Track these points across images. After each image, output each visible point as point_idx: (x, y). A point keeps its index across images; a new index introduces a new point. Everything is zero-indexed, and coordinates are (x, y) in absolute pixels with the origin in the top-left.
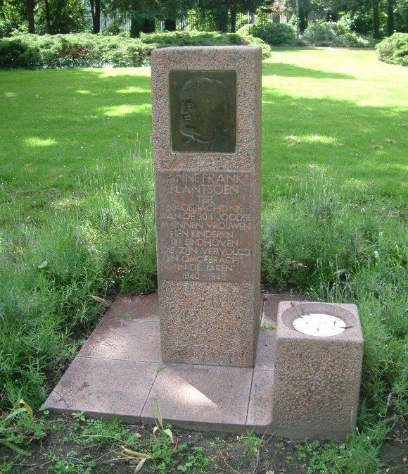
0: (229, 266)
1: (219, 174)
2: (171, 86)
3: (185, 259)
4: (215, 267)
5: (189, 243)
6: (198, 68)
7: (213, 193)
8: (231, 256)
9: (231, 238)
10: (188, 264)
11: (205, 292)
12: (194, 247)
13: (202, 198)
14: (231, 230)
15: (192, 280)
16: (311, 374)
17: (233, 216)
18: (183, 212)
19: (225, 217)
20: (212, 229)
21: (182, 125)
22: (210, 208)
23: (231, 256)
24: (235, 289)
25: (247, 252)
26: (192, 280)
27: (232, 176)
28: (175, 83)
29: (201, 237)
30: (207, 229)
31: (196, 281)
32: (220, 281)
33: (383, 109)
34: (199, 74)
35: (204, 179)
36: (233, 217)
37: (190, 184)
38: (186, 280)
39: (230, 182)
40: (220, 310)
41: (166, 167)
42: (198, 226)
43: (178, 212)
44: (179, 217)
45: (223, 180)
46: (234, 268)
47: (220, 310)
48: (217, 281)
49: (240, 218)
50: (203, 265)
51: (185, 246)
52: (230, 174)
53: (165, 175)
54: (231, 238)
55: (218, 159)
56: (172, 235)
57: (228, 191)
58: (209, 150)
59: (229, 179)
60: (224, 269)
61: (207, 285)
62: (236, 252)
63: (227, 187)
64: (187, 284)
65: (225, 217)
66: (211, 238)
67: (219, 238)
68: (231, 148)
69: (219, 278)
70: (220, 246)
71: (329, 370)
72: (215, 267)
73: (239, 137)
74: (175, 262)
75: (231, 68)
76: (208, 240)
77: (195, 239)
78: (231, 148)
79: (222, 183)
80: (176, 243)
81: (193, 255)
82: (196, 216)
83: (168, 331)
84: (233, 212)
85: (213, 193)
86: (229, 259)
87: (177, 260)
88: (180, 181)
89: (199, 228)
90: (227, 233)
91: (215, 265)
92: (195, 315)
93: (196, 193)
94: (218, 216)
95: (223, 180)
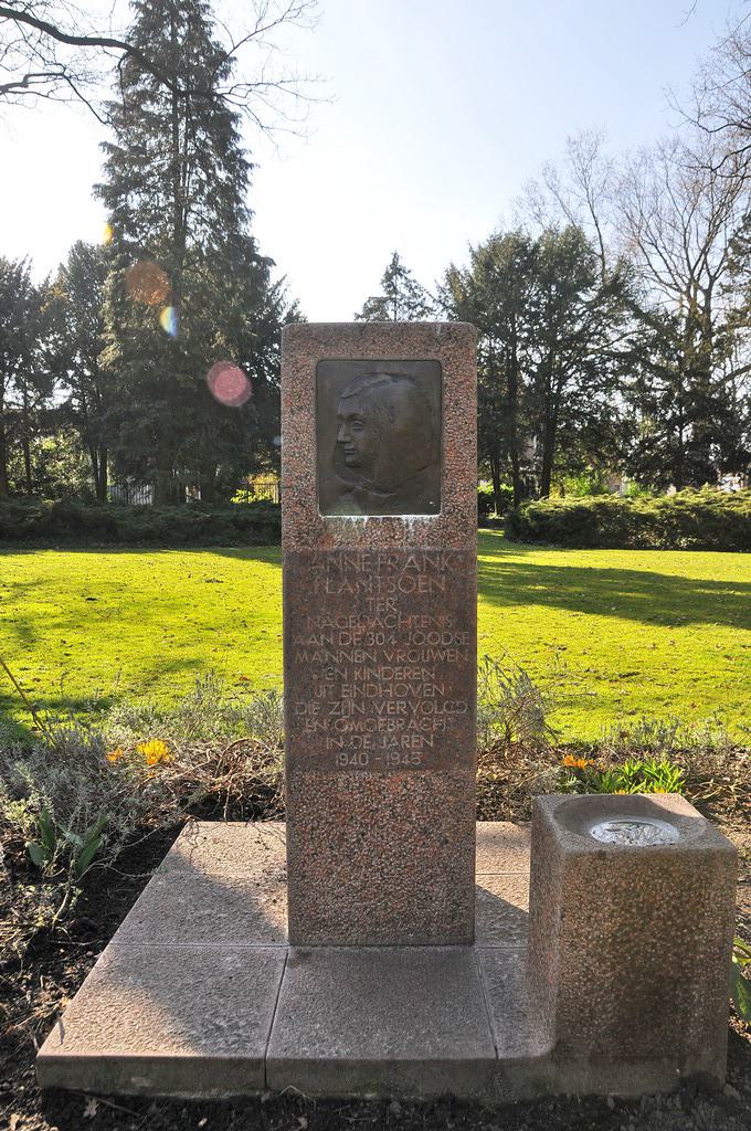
0: (427, 737)
1: (409, 554)
3: (341, 725)
5: (349, 695)
7: (397, 592)
8: (431, 716)
9: (431, 681)
10: (347, 736)
11: (379, 792)
12: (358, 701)
13: (374, 603)
15: (353, 768)
16: (635, 930)
17: (434, 636)
18: (339, 630)
19: (420, 639)
20: (394, 664)
22: (391, 621)
23: (431, 716)
24: (437, 782)
25: (462, 707)
26: (353, 768)
27: (434, 559)
29: (374, 680)
30: (385, 662)
31: (361, 769)
32: (408, 768)
36: (434, 638)
37: (352, 576)
38: (341, 769)
39: (430, 570)
40: (408, 827)
41: (307, 543)
42: (368, 659)
43: (327, 631)
44: (331, 640)
45: (417, 566)
47: (408, 827)
48: (402, 768)
49: (447, 638)
50: (376, 738)
51: (341, 700)
52: (429, 553)
54: (431, 681)
56: (315, 677)
57: (426, 587)
60: (413, 742)
61: (384, 777)
62: (439, 709)
63: (423, 580)
64: (342, 778)
66: (393, 681)
67: (407, 681)
69: (407, 762)
70: (410, 697)
71: (670, 918)
72: (399, 740)
76: (386, 686)
79: (415, 573)
80: (323, 693)
81: (357, 716)
83: (304, 877)
84: (435, 628)
85: (397, 592)
86: (427, 722)
87: (325, 728)
88: (335, 570)
89: (368, 663)
90: (423, 670)
91: (398, 734)
92: (358, 841)
95: (417, 566)
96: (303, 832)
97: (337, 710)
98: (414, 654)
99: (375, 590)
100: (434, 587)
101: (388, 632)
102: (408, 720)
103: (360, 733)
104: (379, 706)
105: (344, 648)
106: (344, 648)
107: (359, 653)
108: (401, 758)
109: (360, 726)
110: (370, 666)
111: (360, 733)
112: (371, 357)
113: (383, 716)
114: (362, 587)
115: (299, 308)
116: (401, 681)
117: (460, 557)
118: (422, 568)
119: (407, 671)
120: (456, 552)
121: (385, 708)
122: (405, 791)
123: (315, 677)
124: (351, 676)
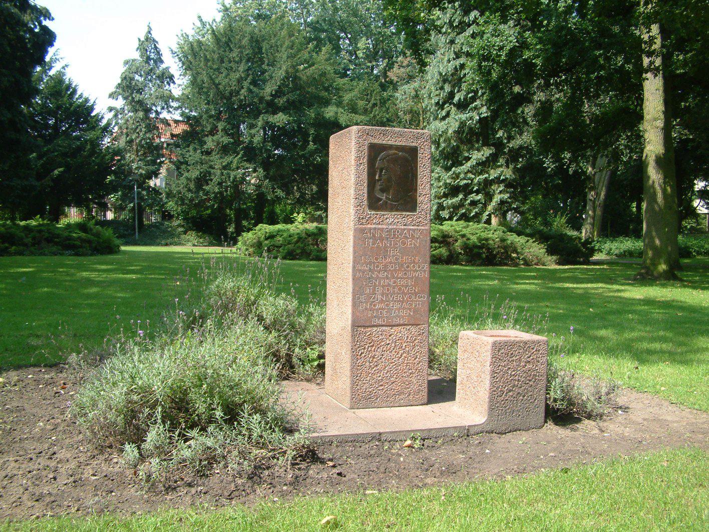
0: (410, 309)
2: (369, 156)
3: (374, 306)
5: (379, 290)
6: (390, 143)
7: (399, 246)
10: (377, 310)
14: (412, 278)
19: (408, 267)
21: (378, 187)
28: (372, 154)
29: (389, 285)
30: (394, 277)
33: (206, 246)
34: (391, 147)
35: (393, 234)
37: (381, 239)
42: (387, 275)
43: (370, 263)
45: (408, 235)
46: (414, 312)
51: (375, 294)
53: (362, 231)
55: (404, 217)
56: (364, 283)
58: (397, 210)
59: (412, 234)
65: (408, 267)
66: (397, 285)
67: (403, 286)
68: (413, 209)
73: (419, 199)
74: (366, 309)
75: (414, 144)
77: (383, 287)
78: (413, 209)
79: (406, 237)
80: (368, 291)
82: (386, 266)
89: (387, 278)
93: (386, 247)
94: (402, 265)
95: (408, 235)
96: (357, 355)
99: (391, 245)
100: (414, 244)
101: (395, 263)
102: (403, 303)
104: (391, 296)
105: (377, 271)
106: (377, 271)
111: (382, 309)
114: (385, 244)
115: (67, 70)
121: (393, 298)
122: (401, 335)
123: (364, 283)
124: (380, 283)
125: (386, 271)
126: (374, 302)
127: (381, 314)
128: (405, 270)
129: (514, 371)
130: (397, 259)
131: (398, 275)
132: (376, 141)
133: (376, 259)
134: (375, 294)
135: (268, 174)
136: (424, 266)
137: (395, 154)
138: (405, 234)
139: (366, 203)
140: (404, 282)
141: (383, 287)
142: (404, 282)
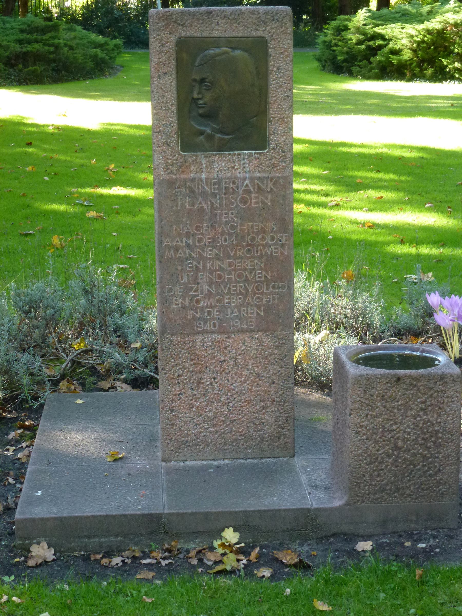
0: (259, 307)
3: (198, 302)
4: (239, 311)
7: (237, 206)
10: (202, 309)
12: (210, 284)
13: (221, 215)
20: (235, 257)
23: (261, 294)
26: (207, 332)
29: (221, 269)
30: (229, 257)
39: (260, 190)
42: (217, 255)
43: (188, 235)
45: (251, 188)
51: (198, 283)
56: (179, 268)
65: (253, 239)
66: (235, 270)
67: (245, 269)
72: (239, 311)
74: (184, 307)
77: (211, 272)
79: (248, 192)
80: (185, 279)
81: (209, 295)
82: (214, 240)
84: (264, 232)
89: (217, 258)
94: (243, 237)
96: (172, 378)
97: (195, 291)
98: (249, 250)
99: (221, 205)
100: (263, 202)
101: (230, 235)
103: (211, 307)
104: (225, 287)
105: (199, 247)
106: (199, 247)
107: (210, 250)
108: (241, 324)
109: (212, 302)
110: (218, 259)
111: (211, 307)
112: (216, 35)
113: (228, 294)
114: (212, 204)
116: (239, 270)
117: (281, 180)
118: (254, 189)
119: (245, 262)
120: (278, 177)
121: (229, 289)
123: (179, 268)
124: (204, 267)
125: (215, 247)
126: (195, 296)
127: (209, 313)
128: (248, 245)
129: (396, 423)
130: (233, 227)
131: (235, 254)
132: (191, 33)
133: (198, 228)
134: (198, 283)
135: (74, 20)
136: (282, 237)
137: (226, 53)
138: (247, 186)
139: (175, 138)
140: (248, 264)
141: (211, 272)
142: (248, 264)
